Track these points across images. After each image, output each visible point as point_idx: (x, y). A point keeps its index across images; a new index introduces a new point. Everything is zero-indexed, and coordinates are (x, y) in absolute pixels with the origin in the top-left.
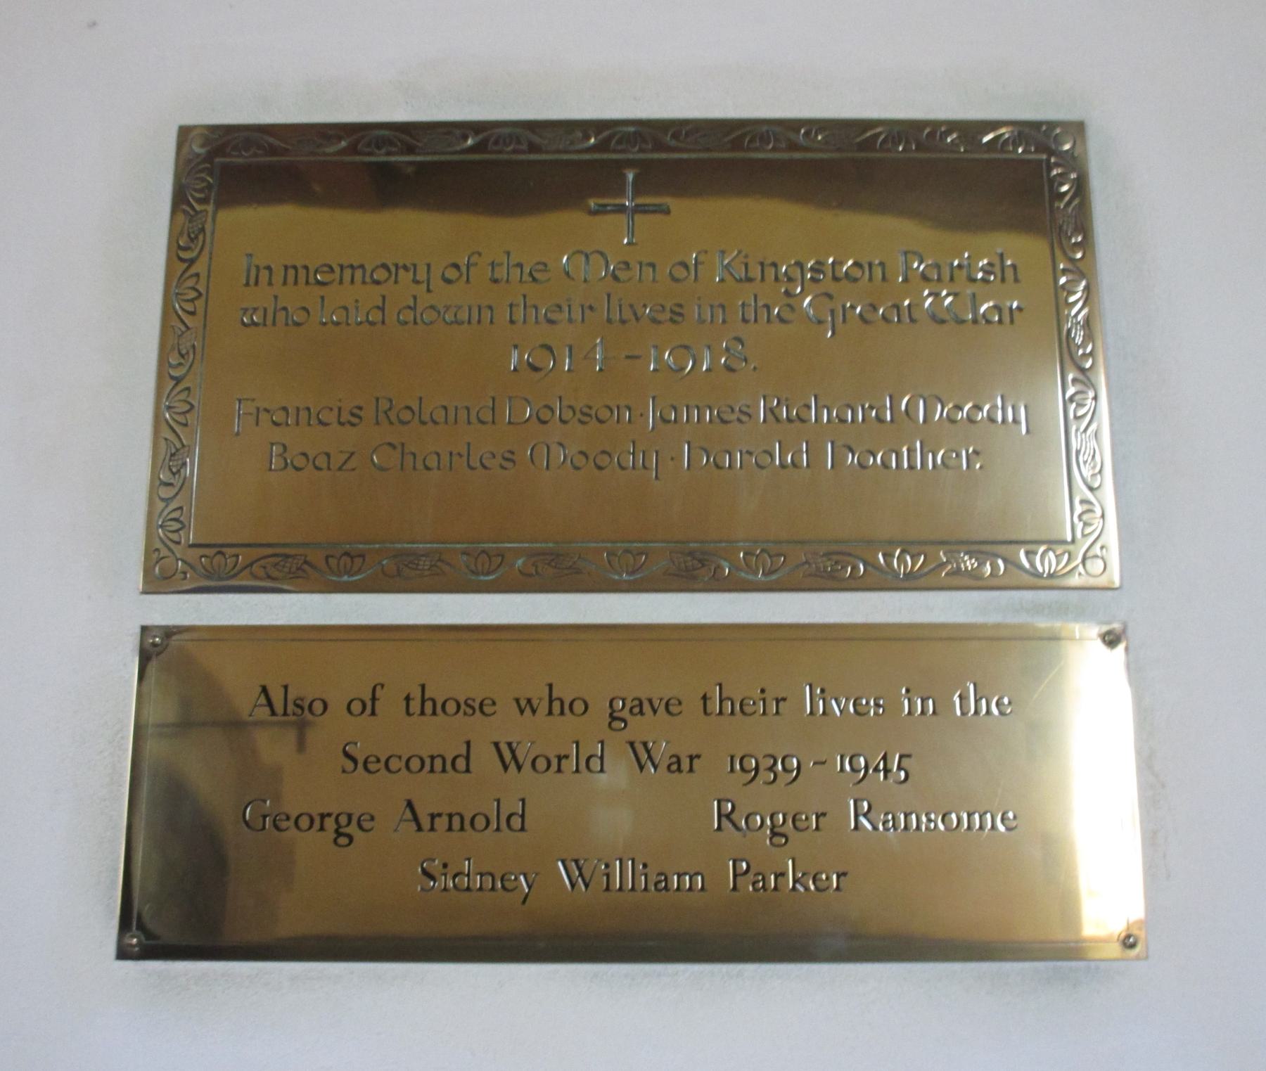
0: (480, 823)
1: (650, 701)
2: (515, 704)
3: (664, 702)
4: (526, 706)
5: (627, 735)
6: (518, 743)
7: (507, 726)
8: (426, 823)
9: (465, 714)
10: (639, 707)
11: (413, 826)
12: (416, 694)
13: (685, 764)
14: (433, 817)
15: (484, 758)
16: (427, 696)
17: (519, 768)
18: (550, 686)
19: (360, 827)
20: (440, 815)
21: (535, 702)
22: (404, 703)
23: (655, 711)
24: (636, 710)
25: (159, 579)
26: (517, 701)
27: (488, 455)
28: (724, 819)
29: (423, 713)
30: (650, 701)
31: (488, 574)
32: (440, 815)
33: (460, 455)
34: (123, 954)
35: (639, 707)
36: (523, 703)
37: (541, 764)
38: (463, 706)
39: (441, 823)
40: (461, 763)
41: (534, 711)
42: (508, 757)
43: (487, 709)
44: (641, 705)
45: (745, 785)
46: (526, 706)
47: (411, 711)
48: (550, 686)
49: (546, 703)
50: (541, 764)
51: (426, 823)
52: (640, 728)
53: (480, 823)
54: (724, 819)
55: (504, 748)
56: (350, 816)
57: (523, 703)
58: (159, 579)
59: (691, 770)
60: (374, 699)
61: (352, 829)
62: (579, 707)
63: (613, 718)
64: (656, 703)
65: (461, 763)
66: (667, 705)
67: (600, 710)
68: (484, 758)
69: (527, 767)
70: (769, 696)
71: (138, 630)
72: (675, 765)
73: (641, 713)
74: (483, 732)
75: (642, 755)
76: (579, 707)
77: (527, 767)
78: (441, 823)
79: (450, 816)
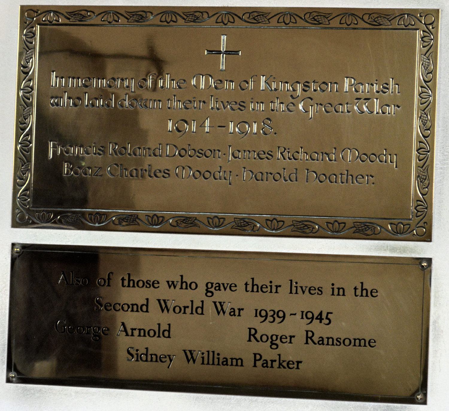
0: (152, 333)
1: (223, 284)
2: (166, 283)
3: (229, 285)
4: (171, 284)
5: (213, 299)
6: (224, 303)
7: (164, 292)
8: (130, 332)
9: (146, 287)
10: (218, 287)
11: (124, 333)
12: (359, 287)
13: (237, 313)
14: (133, 329)
15: (154, 306)
16: (364, 288)
17: (168, 310)
18: (182, 276)
19: (281, 341)
20: (135, 329)
21: (175, 283)
22: (245, 286)
23: (304, 292)
24: (217, 288)
25: (19, 222)
26: (168, 282)
27: (158, 171)
28: (309, 339)
29: (253, 291)
30: (223, 284)
31: (156, 225)
32: (135, 329)
33: (146, 170)
34: (424, 402)
35: (218, 287)
36: (170, 283)
37: (177, 310)
38: (146, 284)
39: (136, 333)
40: (144, 308)
41: (175, 287)
42: (163, 306)
43: (156, 285)
44: (219, 286)
45: (278, 323)
46: (171, 284)
47: (357, 294)
48: (182, 276)
49: (179, 284)
50: (177, 310)
51: (130, 332)
52: (219, 296)
53: (152, 333)
54: (309, 339)
55: (218, 305)
56: (277, 336)
57: (170, 283)
58: (19, 222)
59: (239, 315)
60: (109, 279)
61: (278, 342)
62: (193, 286)
63: (207, 291)
64: (226, 285)
65: (144, 308)
66: (310, 290)
67: (202, 288)
68: (154, 306)
69: (171, 310)
70: (273, 285)
71: (11, 244)
72: (233, 313)
73: (220, 290)
74: (152, 294)
75: (219, 308)
76: (193, 286)
77: (171, 310)
78: (136, 333)
79: (140, 330)
